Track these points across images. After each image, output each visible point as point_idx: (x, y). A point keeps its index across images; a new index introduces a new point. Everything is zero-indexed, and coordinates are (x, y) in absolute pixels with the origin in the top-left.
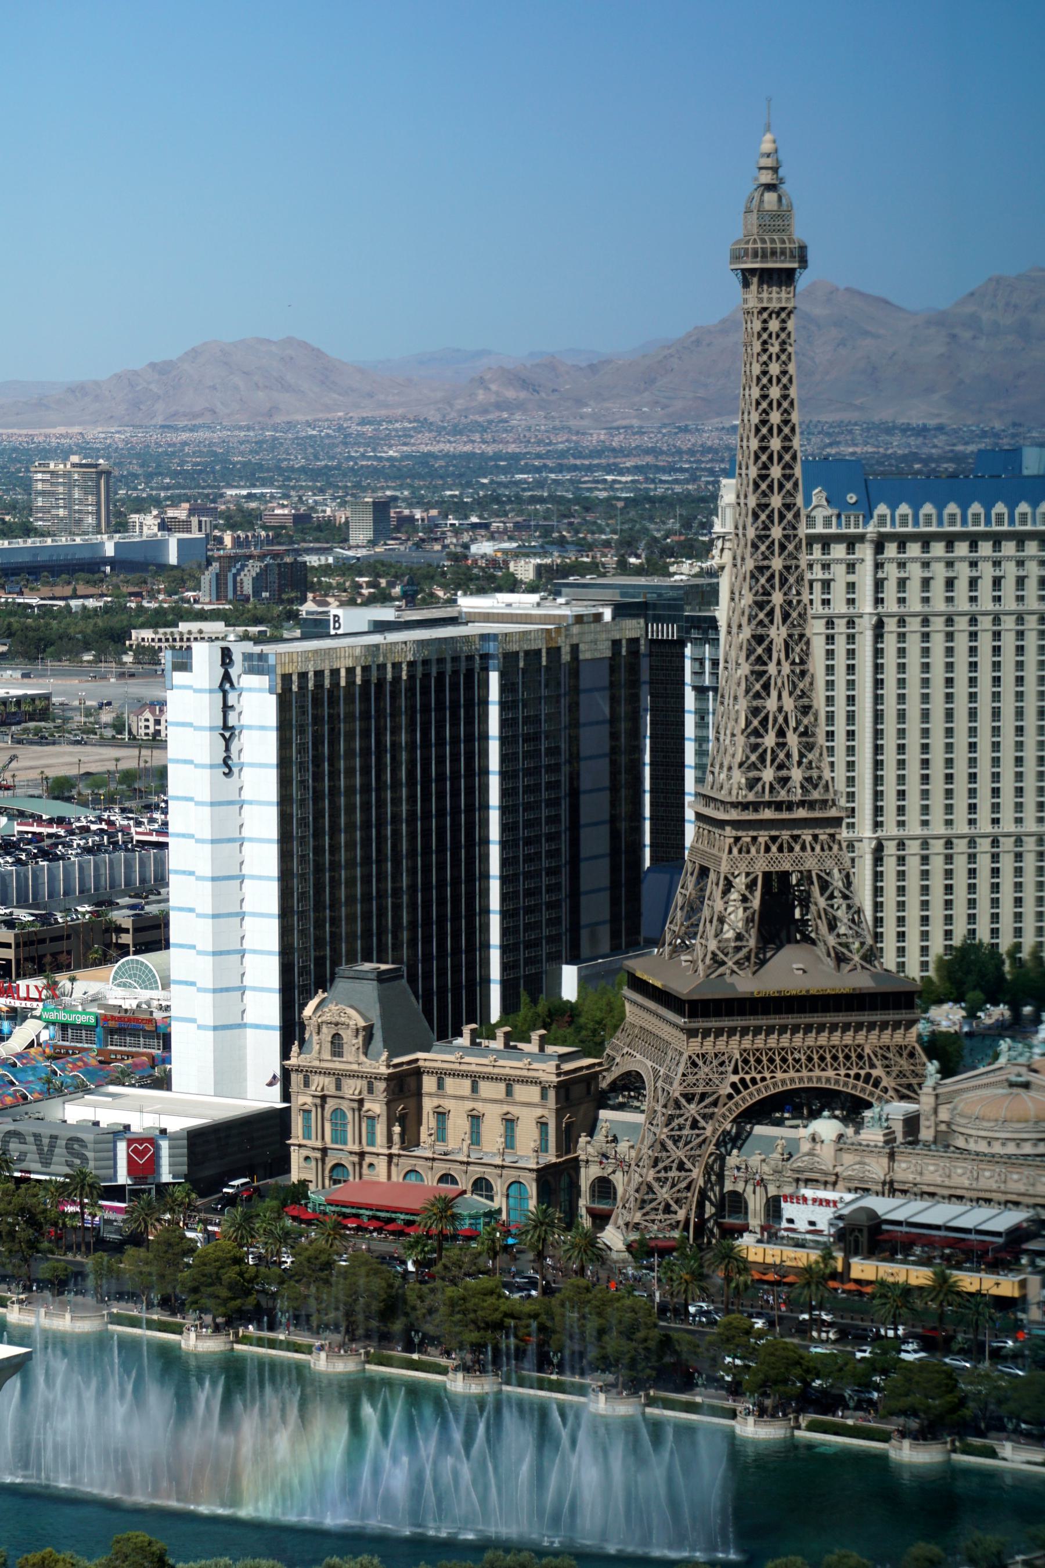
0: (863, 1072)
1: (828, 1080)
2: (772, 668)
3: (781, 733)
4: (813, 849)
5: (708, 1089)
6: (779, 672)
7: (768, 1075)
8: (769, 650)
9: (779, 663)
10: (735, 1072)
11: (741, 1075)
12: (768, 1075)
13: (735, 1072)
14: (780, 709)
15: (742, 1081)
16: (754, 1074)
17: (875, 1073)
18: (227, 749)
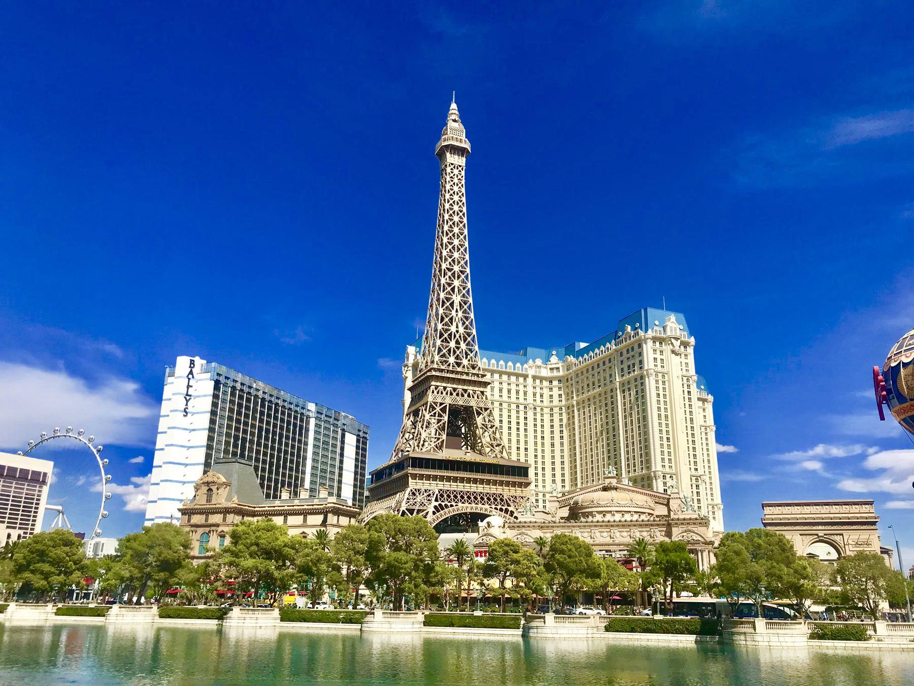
0: (504, 508)
1: (486, 510)
2: (454, 313)
3: (457, 342)
4: (473, 397)
5: (421, 508)
6: (457, 315)
7: (454, 504)
8: (452, 304)
9: (457, 311)
10: (436, 500)
11: (440, 502)
12: (454, 504)
13: (436, 500)
14: (457, 331)
15: (440, 505)
16: (446, 503)
17: (510, 509)
18: (187, 405)
